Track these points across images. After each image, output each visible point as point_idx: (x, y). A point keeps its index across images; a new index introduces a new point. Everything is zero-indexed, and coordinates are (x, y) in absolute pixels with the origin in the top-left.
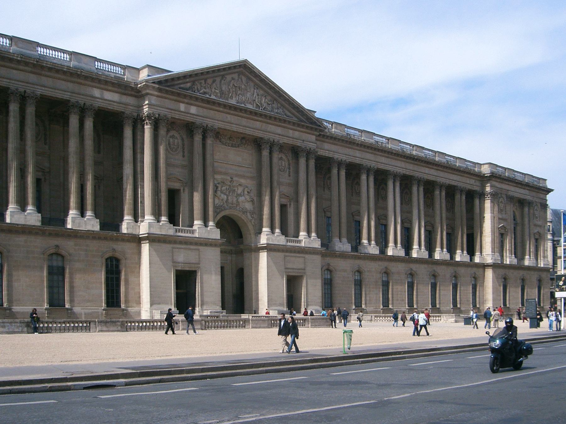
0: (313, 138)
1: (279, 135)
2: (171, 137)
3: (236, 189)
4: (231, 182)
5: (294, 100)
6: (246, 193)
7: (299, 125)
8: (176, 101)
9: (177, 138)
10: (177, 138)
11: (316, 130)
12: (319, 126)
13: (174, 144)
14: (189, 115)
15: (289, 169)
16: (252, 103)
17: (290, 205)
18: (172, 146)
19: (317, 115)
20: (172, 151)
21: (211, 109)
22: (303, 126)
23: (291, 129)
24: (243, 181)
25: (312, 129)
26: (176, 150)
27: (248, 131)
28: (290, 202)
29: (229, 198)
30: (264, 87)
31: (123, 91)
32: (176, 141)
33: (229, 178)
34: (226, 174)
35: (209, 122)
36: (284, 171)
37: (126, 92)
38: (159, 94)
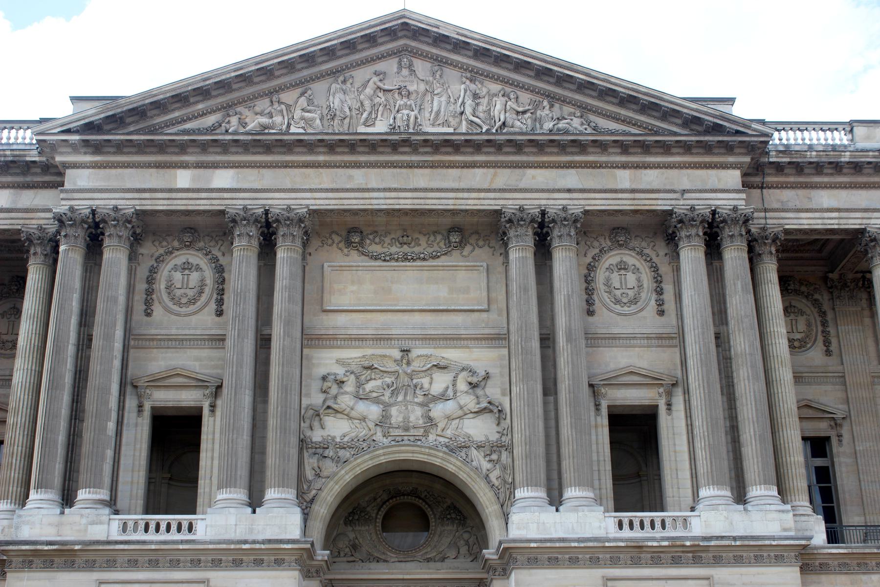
0: (733, 178)
1: (569, 191)
2: (175, 268)
3: (425, 381)
4: (398, 362)
5: (607, 78)
6: (462, 386)
7: (645, 148)
8: (159, 166)
9: (198, 268)
10: (198, 268)
11: (729, 148)
12: (738, 132)
13: (185, 285)
14: (204, 195)
15: (659, 292)
16: (453, 122)
17: (669, 405)
18: (178, 293)
19: (741, 111)
20: (180, 304)
21: (286, 165)
22: (666, 148)
23: (624, 166)
24: (452, 355)
25: (708, 148)
26: (193, 301)
27: (433, 202)
28: (669, 394)
29: (394, 411)
30: (494, 70)
31: (19, 179)
32: (195, 276)
33: (397, 354)
34: (380, 339)
35: (277, 203)
36: (634, 301)
37: (29, 179)
38: (97, 158)
